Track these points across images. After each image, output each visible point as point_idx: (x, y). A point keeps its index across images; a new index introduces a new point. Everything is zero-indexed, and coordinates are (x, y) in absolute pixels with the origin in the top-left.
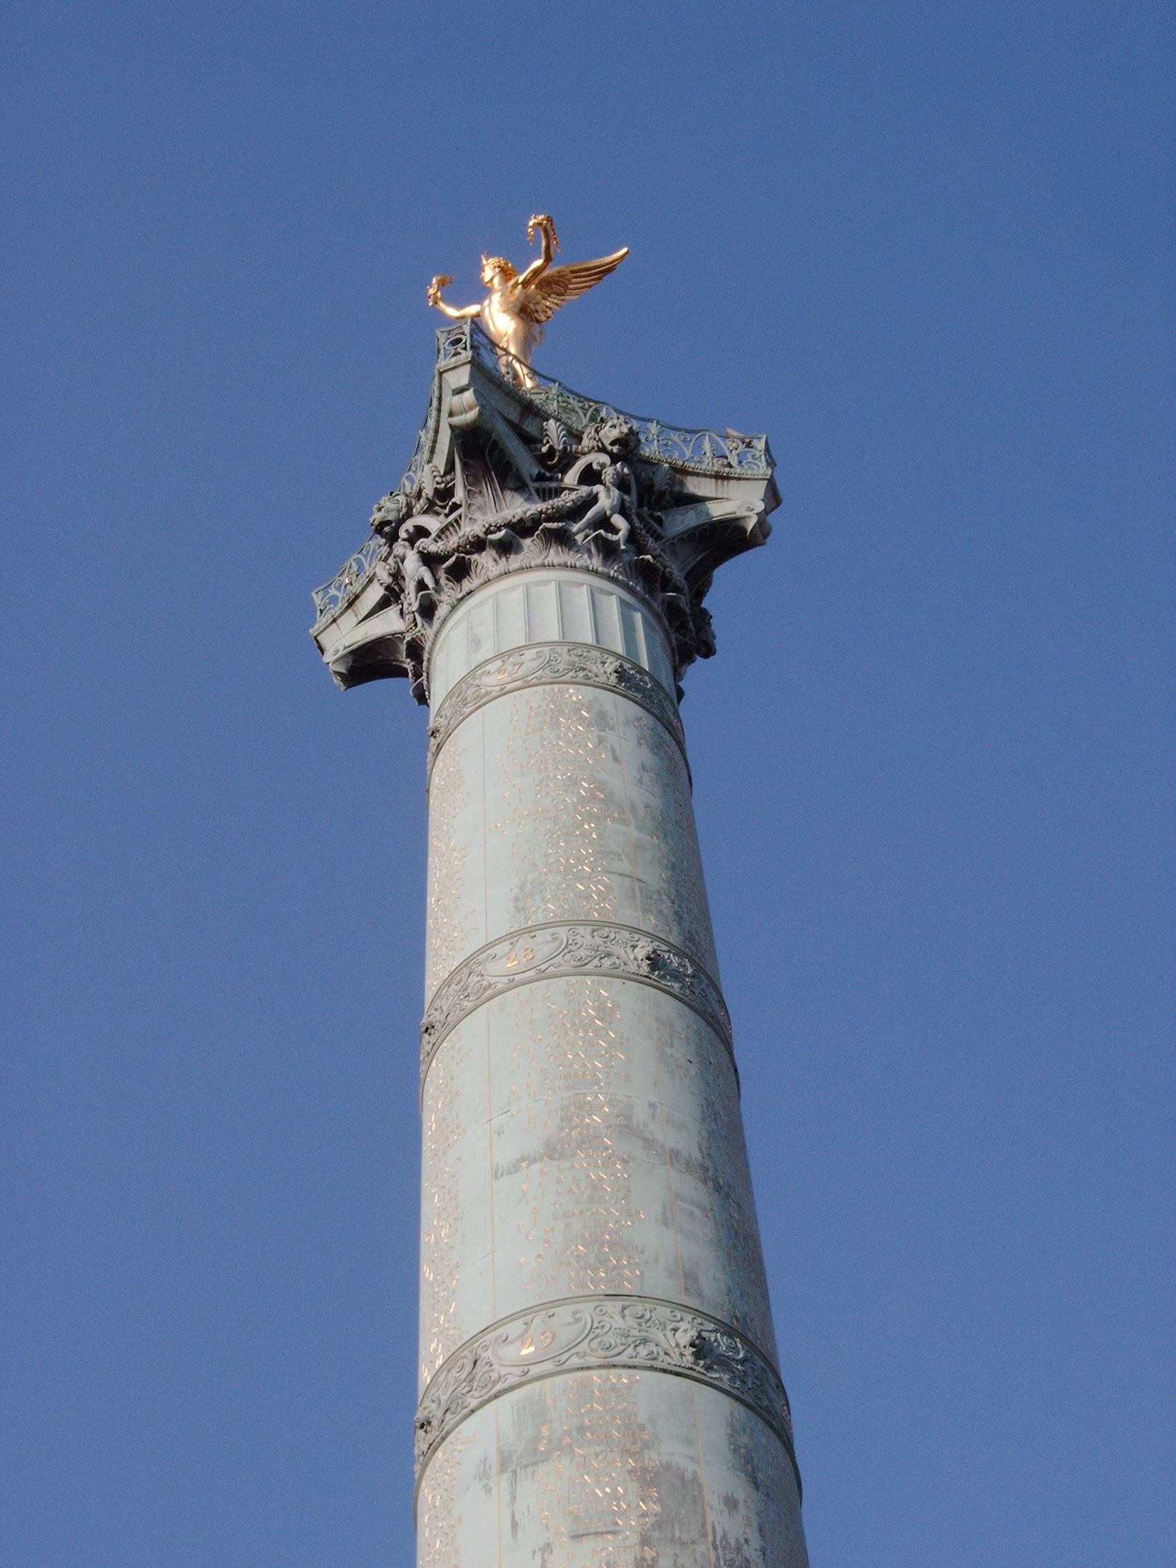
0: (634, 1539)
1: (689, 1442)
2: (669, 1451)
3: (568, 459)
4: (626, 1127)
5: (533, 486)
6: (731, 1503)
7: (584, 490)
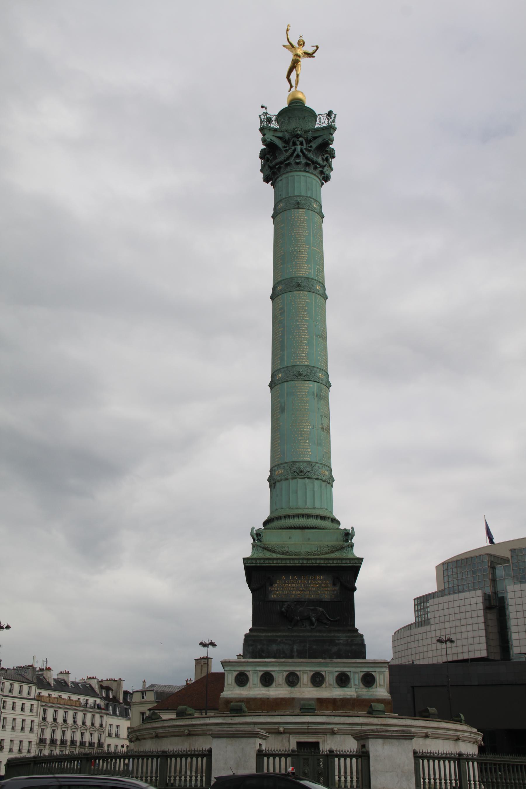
7: (293, 148)
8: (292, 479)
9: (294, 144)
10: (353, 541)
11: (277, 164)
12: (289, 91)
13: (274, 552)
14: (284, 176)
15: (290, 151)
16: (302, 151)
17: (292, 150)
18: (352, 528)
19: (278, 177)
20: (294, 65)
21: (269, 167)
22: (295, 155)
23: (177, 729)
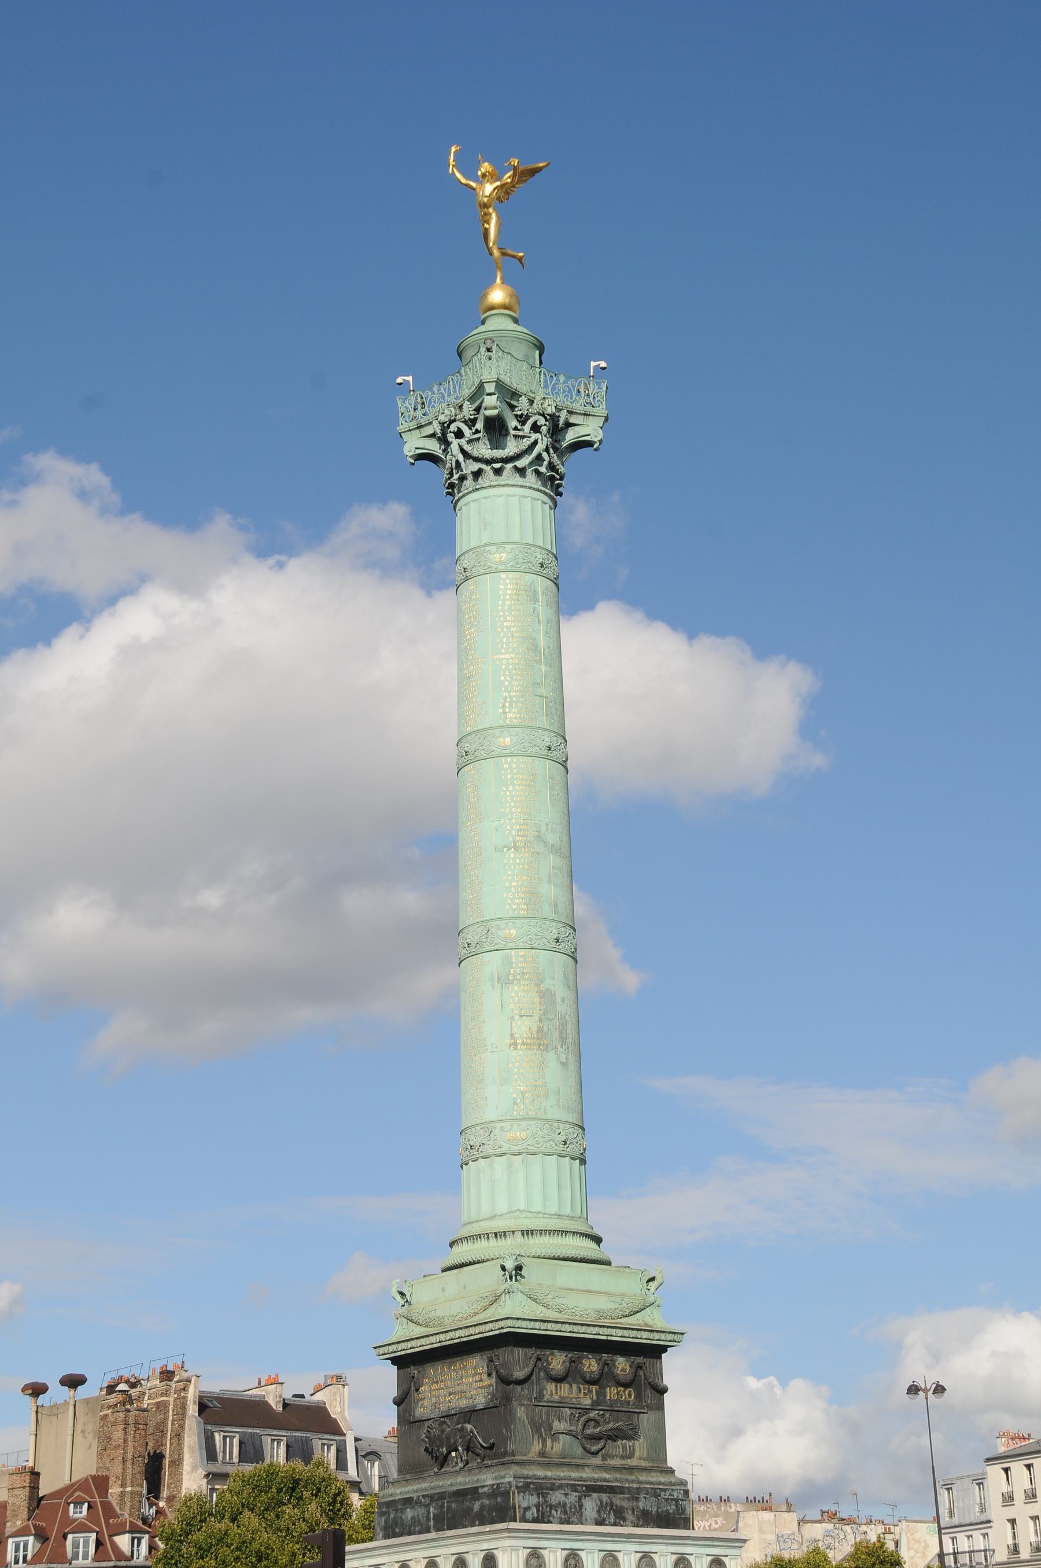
0: (537, 1019)
1: (553, 978)
2: (548, 984)
3: (528, 417)
4: (539, 838)
5: (513, 432)
6: (563, 1000)
7: (535, 436)
9: (535, 428)
15: (527, 442)
16: (547, 450)
17: (532, 440)
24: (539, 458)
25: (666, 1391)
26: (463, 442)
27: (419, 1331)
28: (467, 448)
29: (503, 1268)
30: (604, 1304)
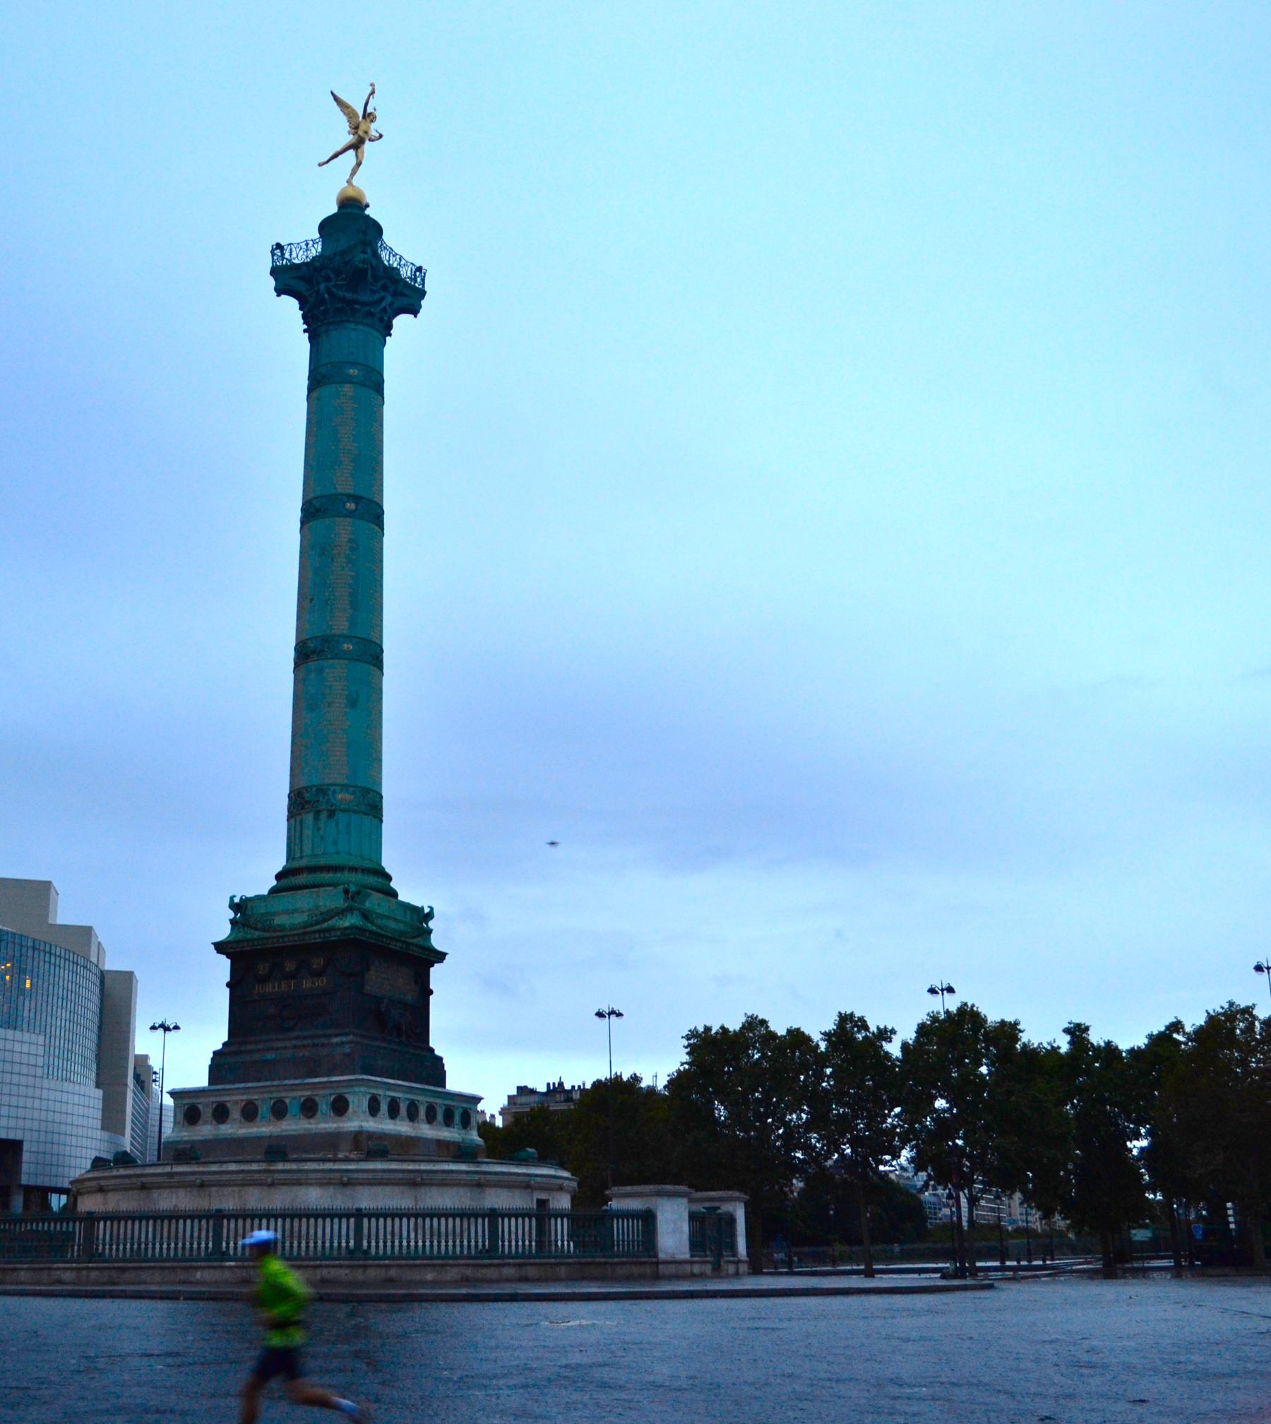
7: (383, 294)
8: (365, 814)
9: (385, 288)
10: (431, 924)
11: (356, 302)
12: (320, 165)
13: (372, 923)
14: (360, 327)
15: (378, 296)
18: (432, 909)
19: (348, 321)
20: (356, 146)
21: (328, 290)
22: (384, 304)
23: (380, 1175)
24: (384, 310)
25: (431, 992)
26: (330, 284)
27: (257, 934)
28: (334, 290)
29: (346, 892)
30: (401, 927)
